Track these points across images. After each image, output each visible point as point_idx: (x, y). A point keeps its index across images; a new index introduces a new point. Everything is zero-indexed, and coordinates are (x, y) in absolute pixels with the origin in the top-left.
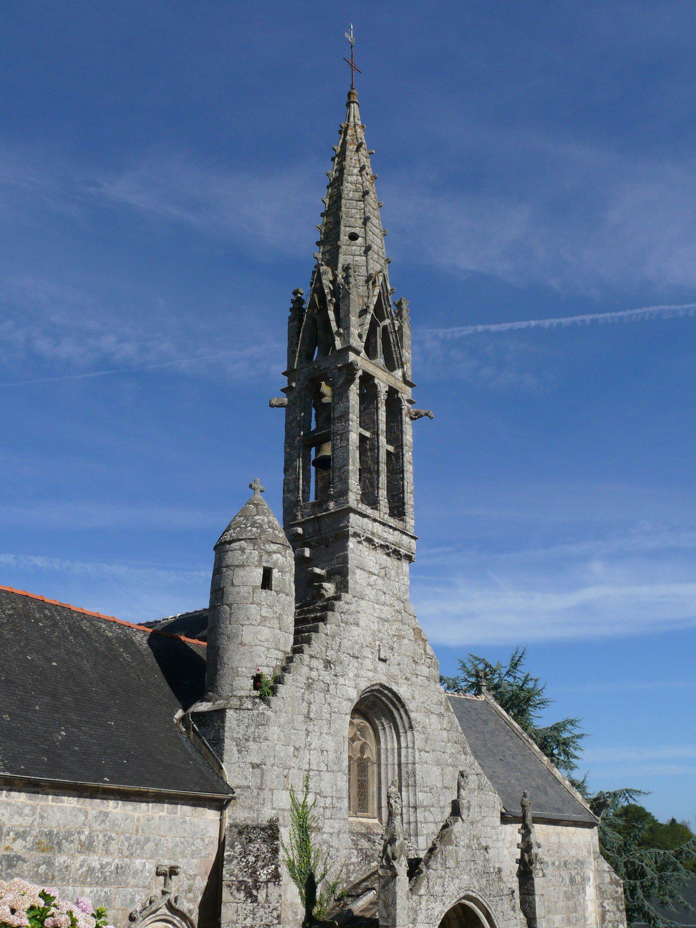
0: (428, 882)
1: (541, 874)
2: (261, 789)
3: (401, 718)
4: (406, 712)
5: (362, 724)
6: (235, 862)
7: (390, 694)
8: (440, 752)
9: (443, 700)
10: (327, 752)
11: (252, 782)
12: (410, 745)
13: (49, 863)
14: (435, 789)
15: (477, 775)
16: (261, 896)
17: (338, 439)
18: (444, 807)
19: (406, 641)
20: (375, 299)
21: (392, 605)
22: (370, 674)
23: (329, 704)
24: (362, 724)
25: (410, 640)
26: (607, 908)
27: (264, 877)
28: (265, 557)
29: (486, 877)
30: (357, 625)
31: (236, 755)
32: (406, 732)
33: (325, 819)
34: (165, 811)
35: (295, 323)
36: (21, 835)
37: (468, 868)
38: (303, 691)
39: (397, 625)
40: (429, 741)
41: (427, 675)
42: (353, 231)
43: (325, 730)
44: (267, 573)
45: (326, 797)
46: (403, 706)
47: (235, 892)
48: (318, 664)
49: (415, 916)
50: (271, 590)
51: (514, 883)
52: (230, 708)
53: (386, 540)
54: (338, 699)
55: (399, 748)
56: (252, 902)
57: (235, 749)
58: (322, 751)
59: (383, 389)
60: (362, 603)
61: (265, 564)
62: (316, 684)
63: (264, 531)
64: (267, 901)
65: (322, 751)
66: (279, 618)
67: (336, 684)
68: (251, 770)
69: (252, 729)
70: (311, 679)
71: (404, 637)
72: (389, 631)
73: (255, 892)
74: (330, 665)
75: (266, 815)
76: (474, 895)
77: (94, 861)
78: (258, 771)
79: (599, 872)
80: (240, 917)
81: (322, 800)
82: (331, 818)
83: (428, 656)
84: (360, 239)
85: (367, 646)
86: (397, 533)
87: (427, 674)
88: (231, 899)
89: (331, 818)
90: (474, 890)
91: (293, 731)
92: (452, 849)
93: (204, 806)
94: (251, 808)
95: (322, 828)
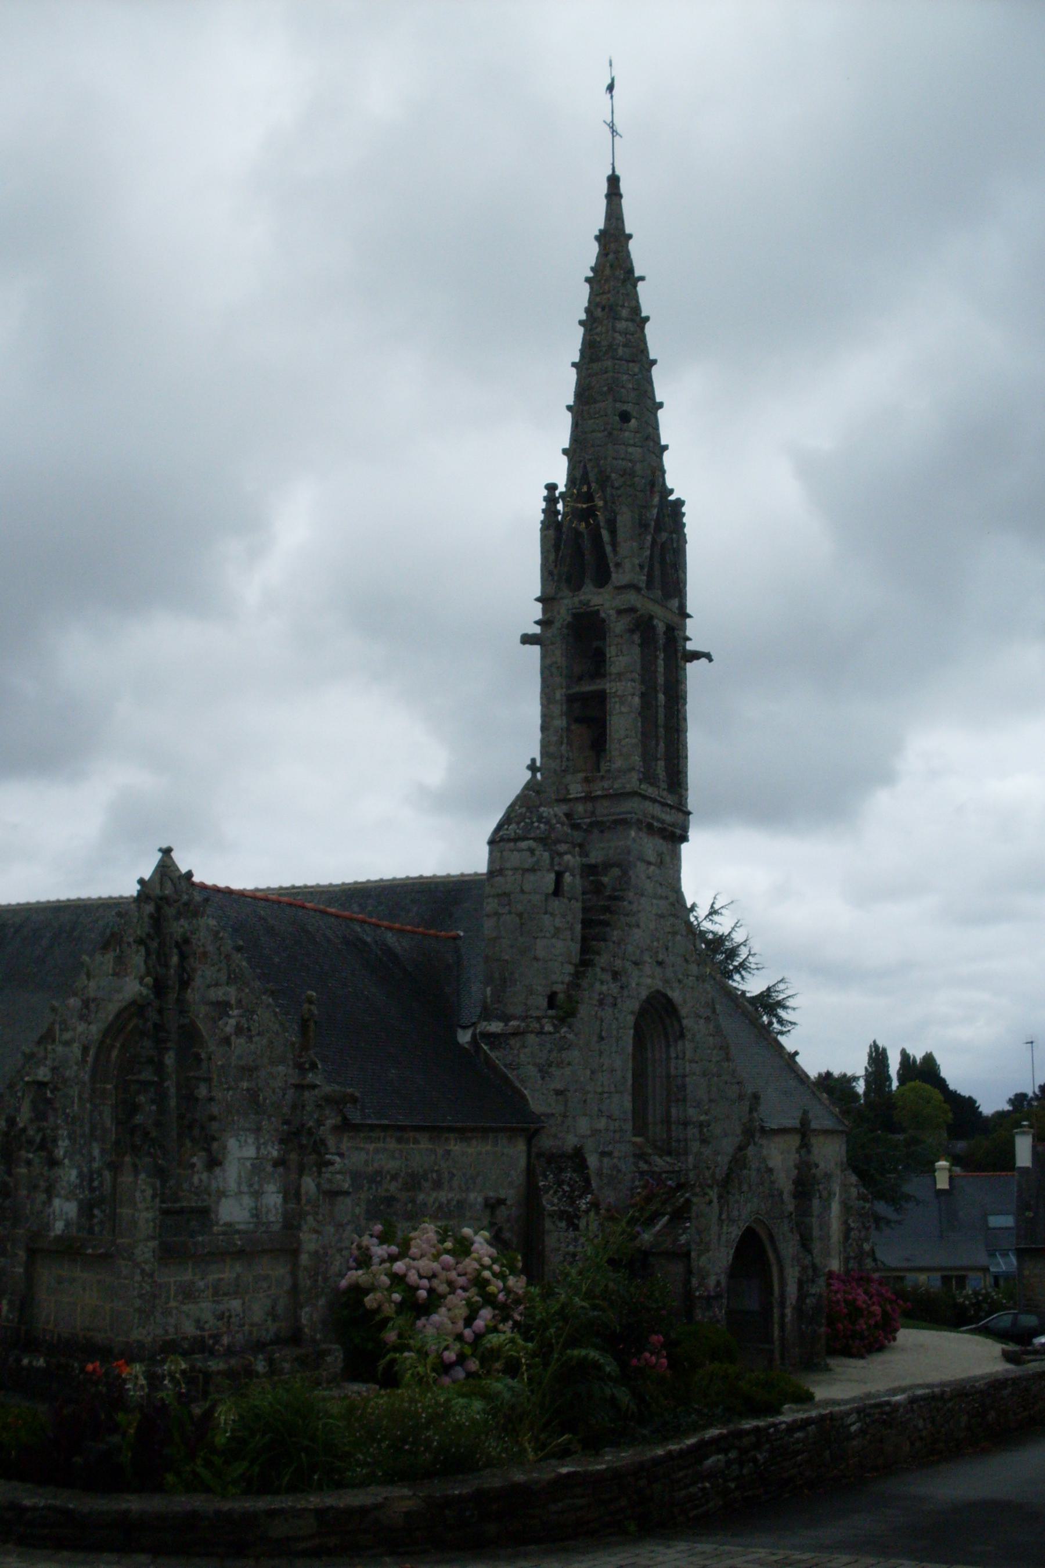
0: (728, 1207)
1: (818, 1195)
2: (565, 1116)
6: (551, 1192)
12: (681, 1055)
13: (413, 1201)
16: (582, 1224)
17: (616, 702)
19: (679, 937)
20: (655, 511)
21: (667, 898)
22: (649, 981)
25: (682, 936)
26: (852, 1225)
27: (584, 1206)
28: (557, 860)
30: (638, 926)
31: (540, 1082)
35: (551, 532)
36: (394, 1178)
39: (672, 919)
42: (624, 408)
44: (559, 876)
45: (616, 1120)
48: (607, 977)
50: (564, 897)
51: (790, 1205)
52: (532, 1032)
53: (663, 822)
55: (669, 1058)
56: (573, 1230)
59: (661, 627)
60: (643, 900)
61: (556, 868)
63: (552, 828)
66: (571, 929)
68: (554, 1097)
69: (555, 1054)
73: (576, 1221)
75: (571, 1141)
76: (761, 1218)
77: (443, 1196)
79: (845, 1186)
80: (563, 1244)
84: (633, 421)
85: (646, 950)
86: (673, 811)
91: (590, 1053)
94: (555, 1136)
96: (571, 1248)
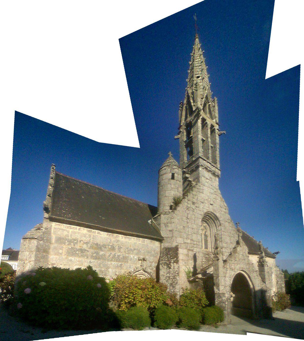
2: (173, 237)
3: (217, 223)
11: (170, 235)
19: (218, 201)
22: (207, 208)
32: (219, 227)
34: (141, 242)
43: (193, 222)
46: (218, 219)
47: (164, 266)
57: (164, 227)
58: (192, 229)
61: (172, 172)
64: (174, 269)
68: (169, 232)
71: (217, 199)
75: (174, 245)
78: (171, 232)
87: (224, 211)
88: (162, 268)
96: (168, 275)
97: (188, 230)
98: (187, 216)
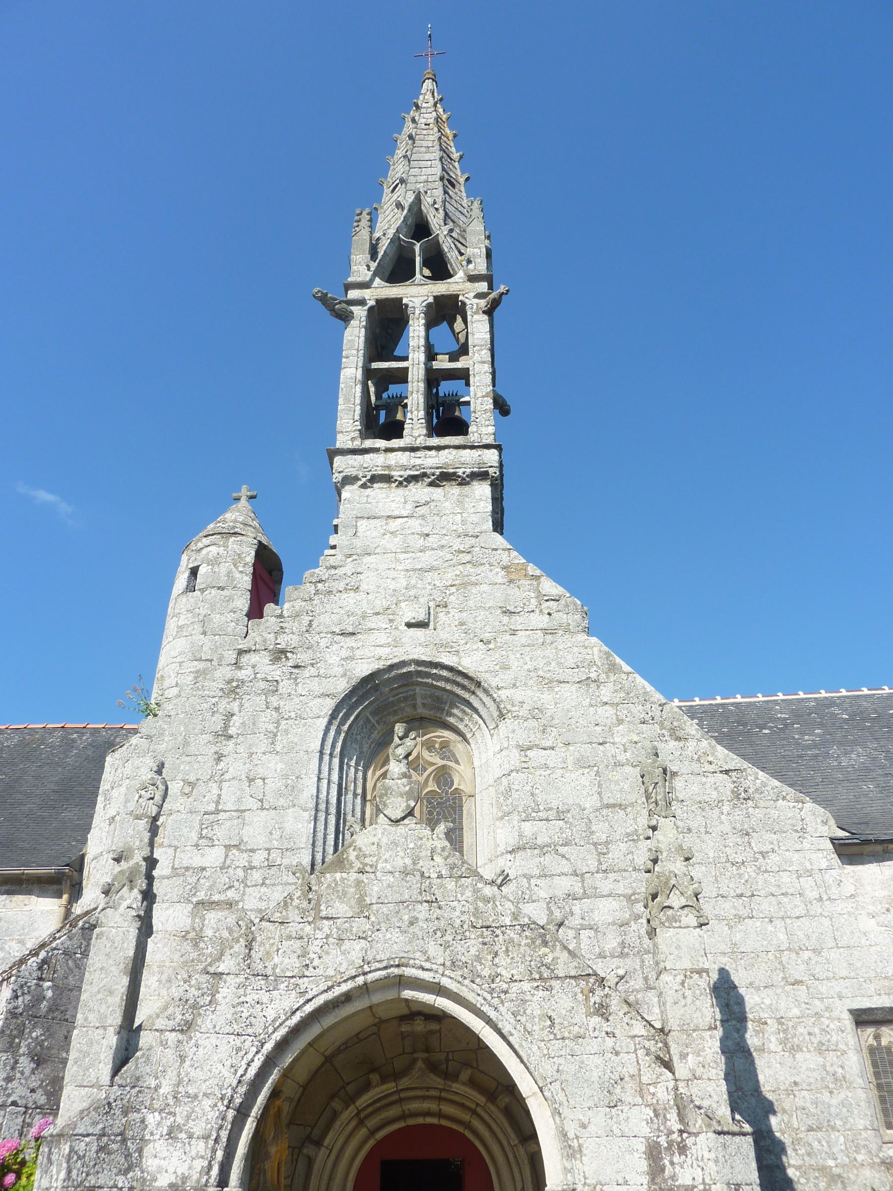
4: (486, 691)
5: (439, 740)
7: (445, 673)
8: (591, 743)
9: (596, 657)
10: (264, 779)
14: (575, 811)
15: (727, 772)
18: (607, 843)
23: (277, 709)
24: (439, 740)
29: (482, 936)
33: (246, 886)
37: (406, 917)
38: (214, 700)
40: (549, 729)
41: (545, 627)
46: (479, 684)
49: (189, 1017)
54: (296, 700)
58: (251, 780)
62: (247, 687)
65: (251, 780)
67: (296, 679)
70: (238, 680)
72: (437, 583)
74: (285, 655)
81: (245, 855)
82: (263, 884)
83: (546, 598)
85: (378, 614)
89: (263, 884)
90: (427, 965)
92: (343, 879)
93: (29, 893)
95: (237, 902)
97: (215, 791)
98: (219, 726)
